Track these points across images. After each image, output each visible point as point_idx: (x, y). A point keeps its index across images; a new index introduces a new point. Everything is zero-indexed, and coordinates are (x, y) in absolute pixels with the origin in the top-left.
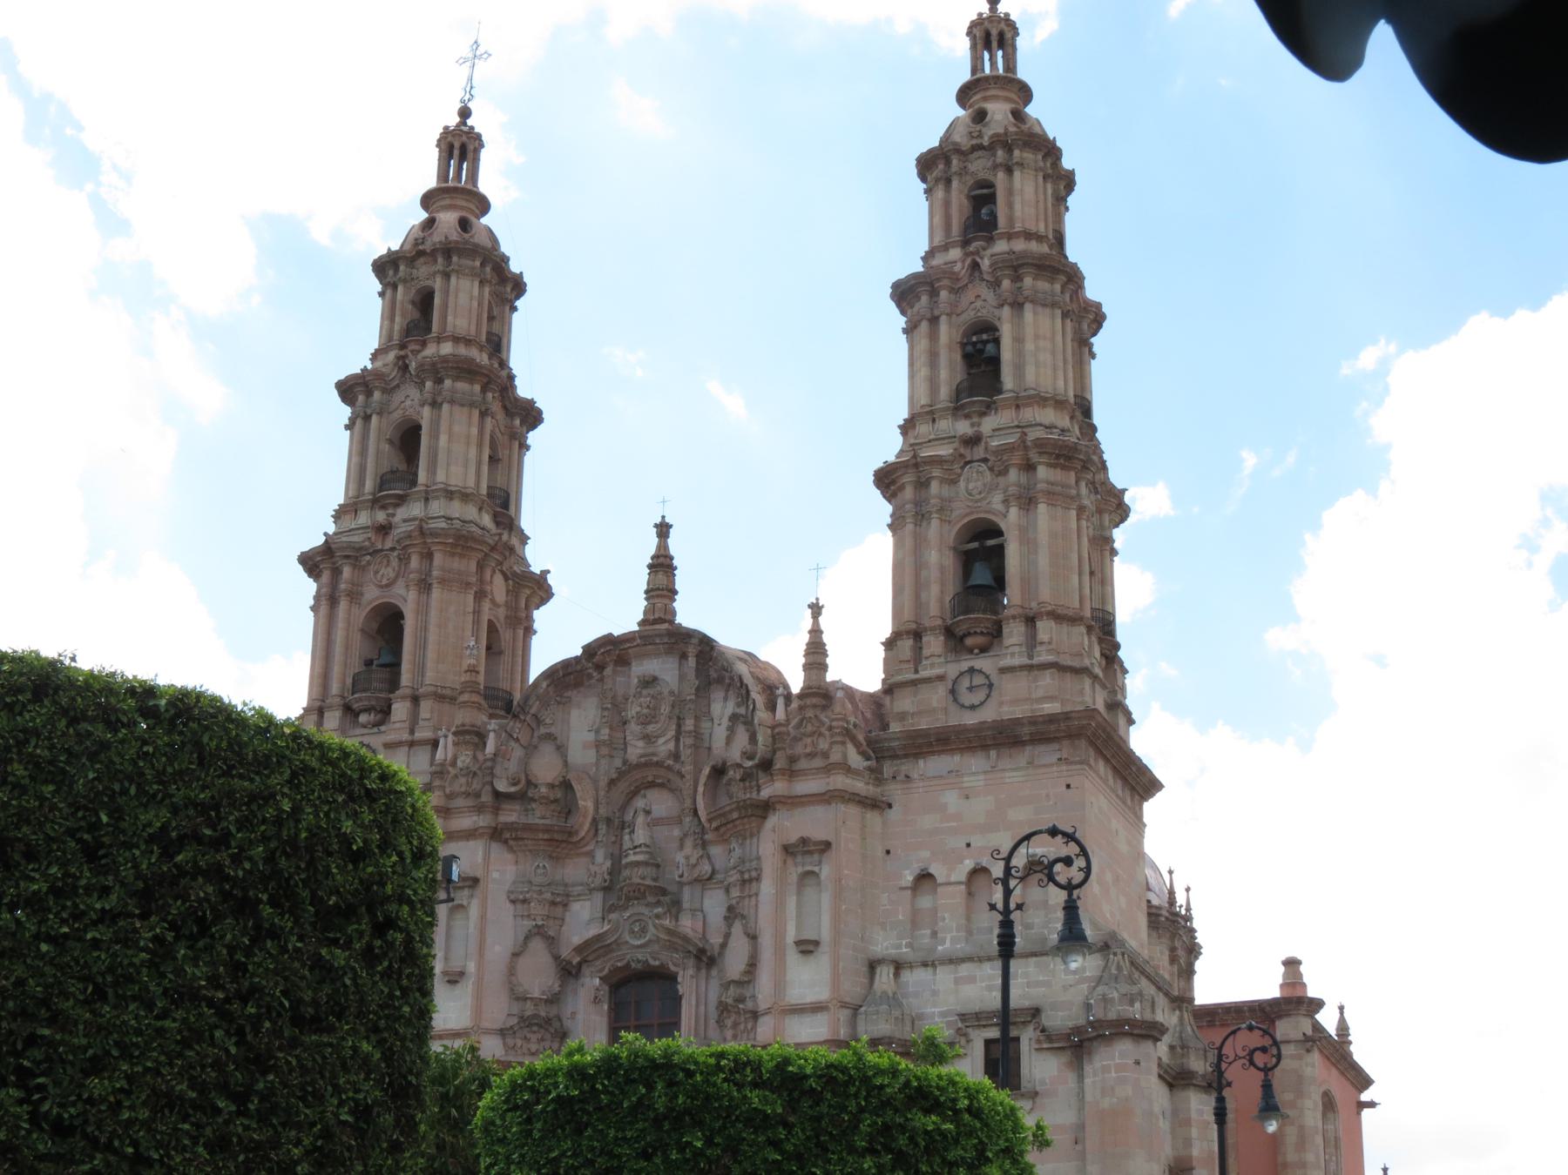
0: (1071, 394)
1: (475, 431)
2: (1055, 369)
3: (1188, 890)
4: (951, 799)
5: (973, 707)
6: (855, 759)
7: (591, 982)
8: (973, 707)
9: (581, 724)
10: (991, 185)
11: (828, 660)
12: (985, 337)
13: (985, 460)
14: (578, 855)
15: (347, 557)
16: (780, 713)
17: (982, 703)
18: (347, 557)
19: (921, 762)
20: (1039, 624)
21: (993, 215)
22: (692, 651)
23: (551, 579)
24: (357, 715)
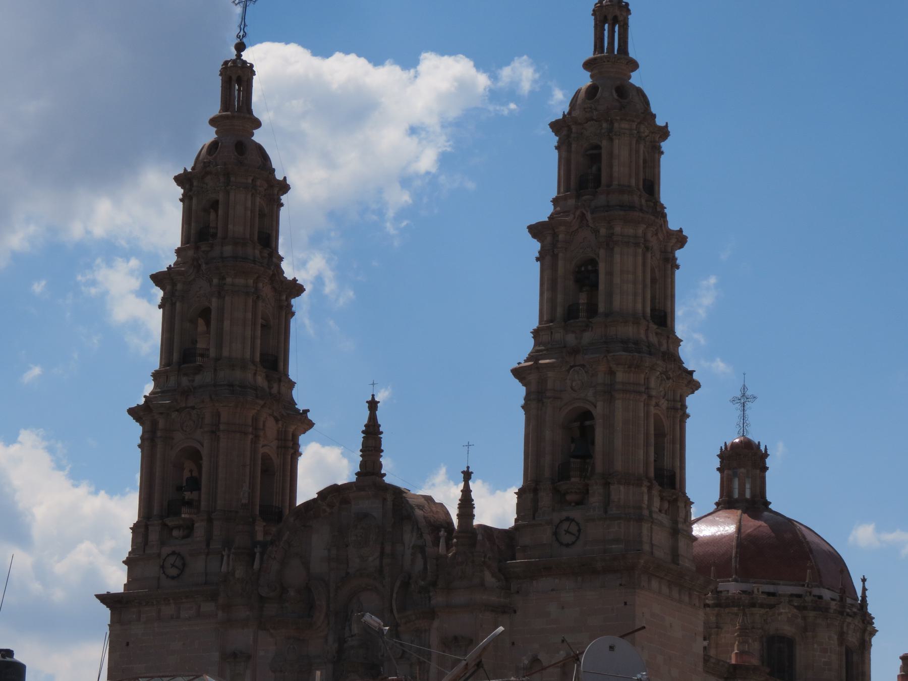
0: (648, 310)
1: (249, 315)
2: (635, 295)
3: (864, 580)
5: (567, 545)
6: (489, 579)
8: (567, 545)
9: (319, 543)
10: (598, 147)
11: (476, 512)
12: (590, 268)
13: (583, 366)
15: (161, 413)
16: (442, 549)
17: (573, 543)
18: (161, 413)
19: (534, 582)
20: (612, 487)
21: (599, 170)
22: (389, 497)
23: (310, 416)
24: (171, 529)
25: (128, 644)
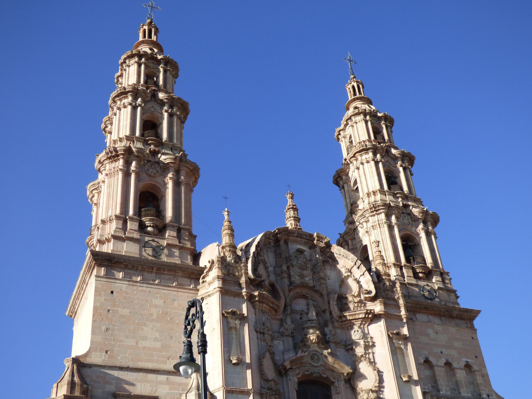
4: (430, 331)
7: (293, 380)
14: (274, 319)
19: (417, 315)
25: (112, 292)
